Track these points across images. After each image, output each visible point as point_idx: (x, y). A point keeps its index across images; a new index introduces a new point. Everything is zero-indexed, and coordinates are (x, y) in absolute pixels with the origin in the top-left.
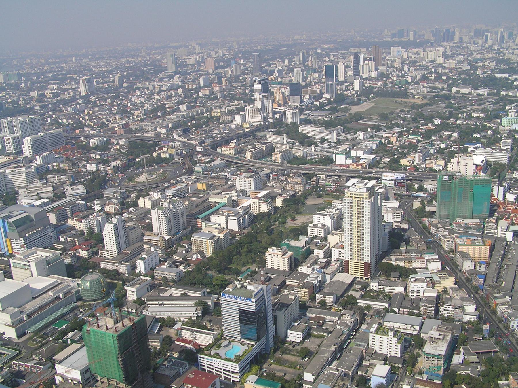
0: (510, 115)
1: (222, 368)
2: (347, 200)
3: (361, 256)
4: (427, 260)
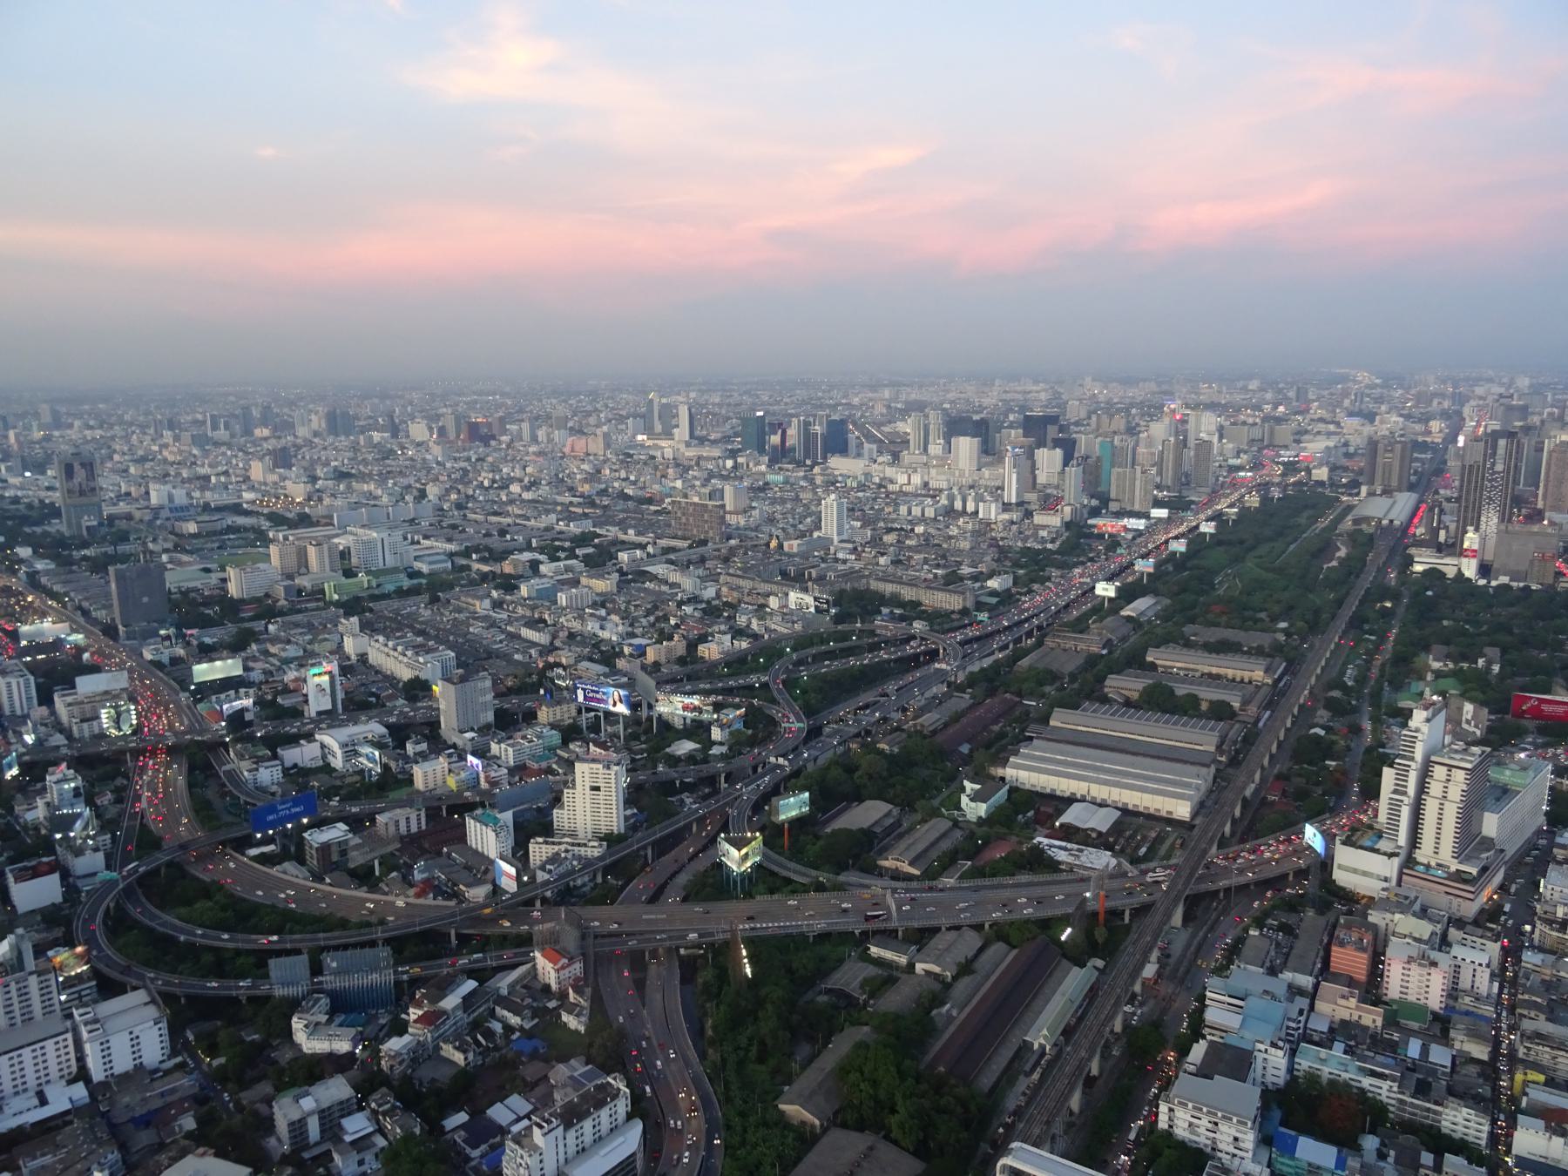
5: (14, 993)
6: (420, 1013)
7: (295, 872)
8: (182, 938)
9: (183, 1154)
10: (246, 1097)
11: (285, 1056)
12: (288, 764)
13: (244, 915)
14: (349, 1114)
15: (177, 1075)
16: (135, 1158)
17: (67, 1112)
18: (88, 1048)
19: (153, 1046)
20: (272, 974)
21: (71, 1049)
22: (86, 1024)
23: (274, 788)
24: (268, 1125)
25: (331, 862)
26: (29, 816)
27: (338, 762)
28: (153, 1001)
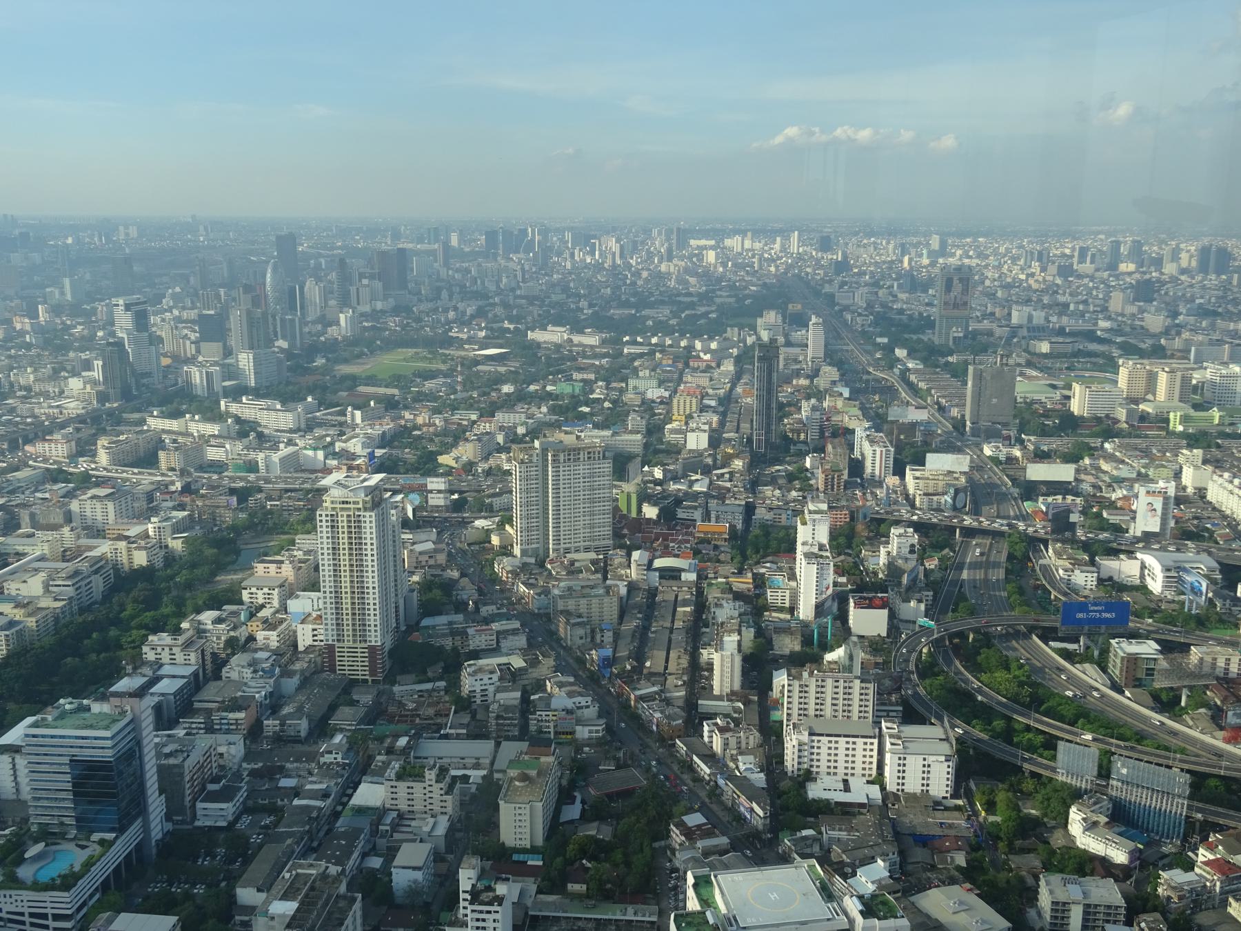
0: (641, 374)
1: (27, 911)
4: (498, 633)
5: (841, 690)
6: (1212, 857)
7: (1095, 676)
8: (979, 698)
9: (952, 881)
10: (1015, 861)
11: (1057, 840)
12: (1104, 575)
14: (1115, 922)
15: (956, 814)
16: (910, 868)
17: (862, 805)
18: (888, 756)
19: (940, 781)
20: (1060, 756)
21: (875, 753)
22: (891, 736)
24: (1031, 895)
27: (1156, 585)
28: (947, 740)
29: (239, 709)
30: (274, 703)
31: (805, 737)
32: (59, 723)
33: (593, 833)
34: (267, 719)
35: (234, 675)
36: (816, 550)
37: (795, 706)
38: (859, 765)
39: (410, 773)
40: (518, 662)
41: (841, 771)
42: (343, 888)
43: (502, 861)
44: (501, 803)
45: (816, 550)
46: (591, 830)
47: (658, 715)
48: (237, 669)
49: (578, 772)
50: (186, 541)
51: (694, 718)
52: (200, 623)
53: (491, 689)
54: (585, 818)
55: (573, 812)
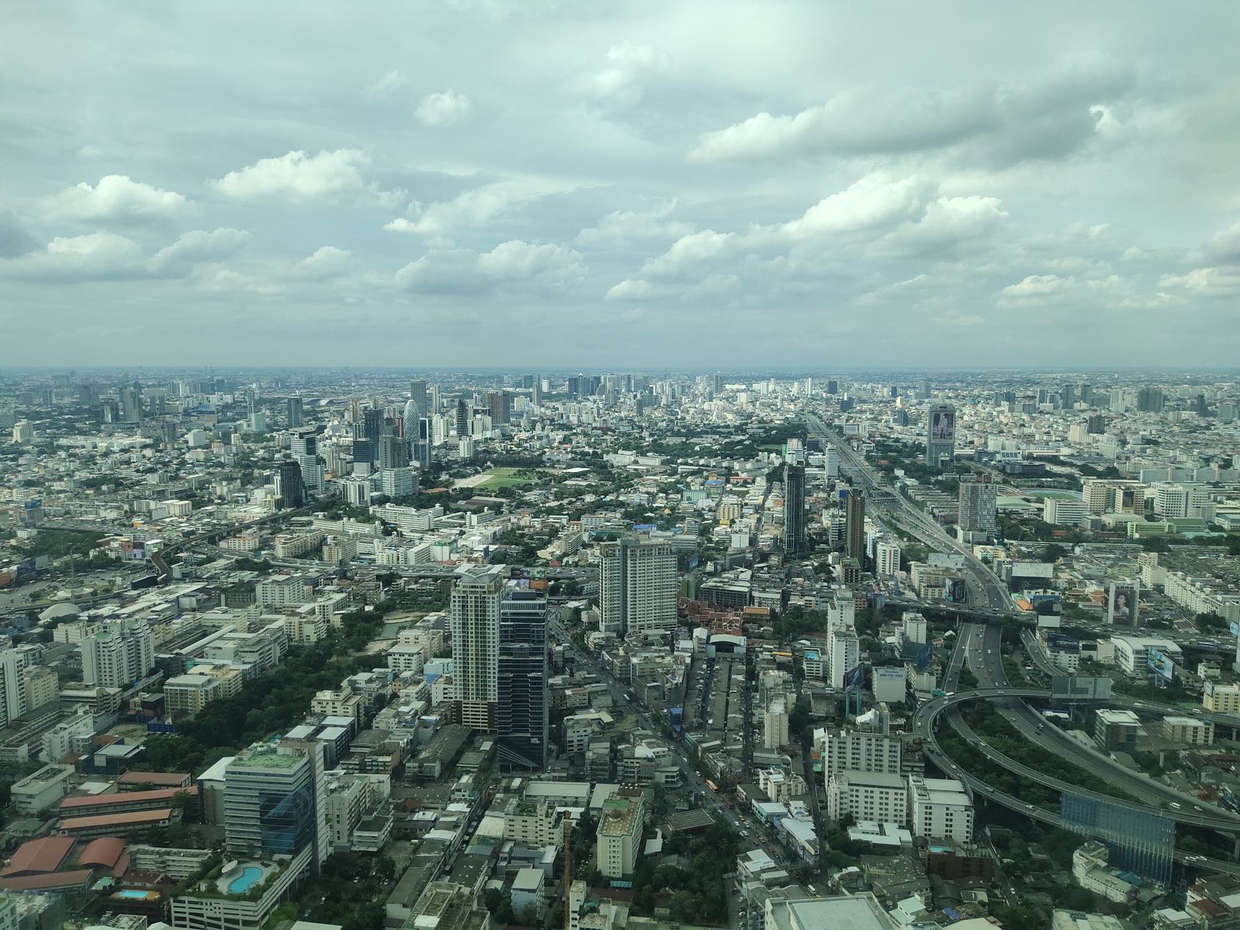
1: (223, 917)
2: (455, 606)
3: (482, 691)
5: (873, 747)
9: (977, 915)
13: (1039, 759)
23: (1072, 670)
25: (1118, 739)
26: (889, 640)
28: (965, 792)
29: (388, 754)
30: (413, 750)
31: (845, 788)
32: (252, 762)
33: (674, 864)
34: (409, 761)
35: (383, 726)
36: (844, 629)
37: (835, 759)
38: (891, 812)
39: (527, 808)
40: (607, 718)
41: (876, 816)
42: (475, 907)
43: (599, 884)
44: (599, 836)
45: (844, 629)
46: (673, 861)
47: (721, 764)
48: (385, 718)
49: (659, 809)
50: (345, 618)
51: (751, 767)
52: (356, 682)
53: (586, 739)
54: (667, 850)
55: (655, 845)
